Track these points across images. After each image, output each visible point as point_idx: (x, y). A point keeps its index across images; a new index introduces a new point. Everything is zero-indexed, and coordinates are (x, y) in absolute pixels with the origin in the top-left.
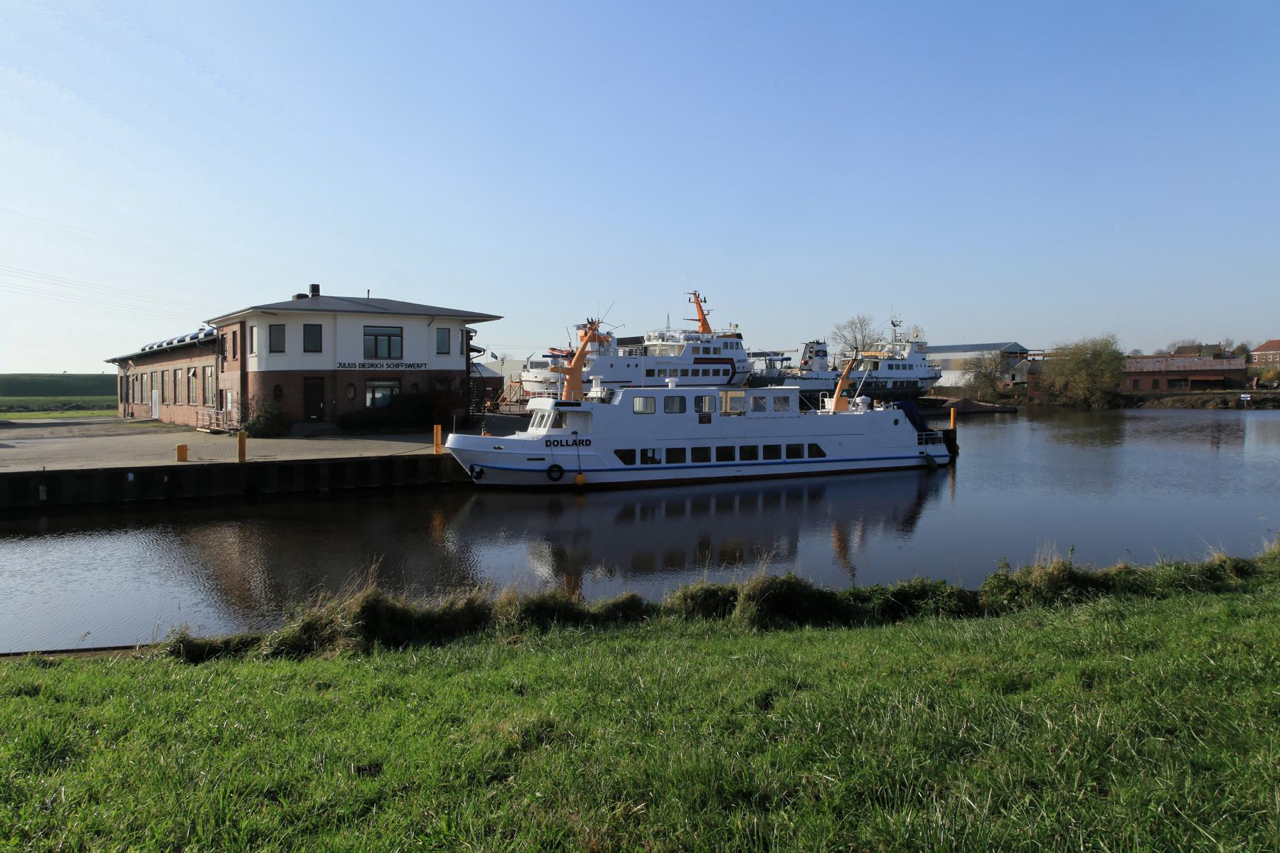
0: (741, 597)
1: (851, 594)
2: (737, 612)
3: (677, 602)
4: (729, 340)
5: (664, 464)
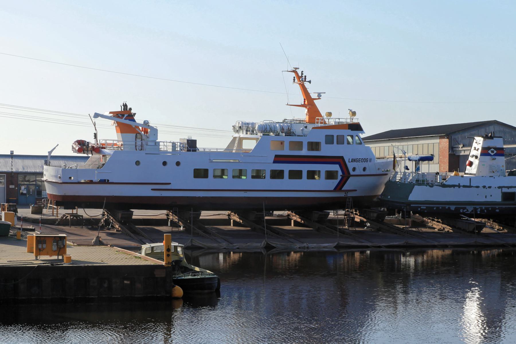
4: (335, 133)
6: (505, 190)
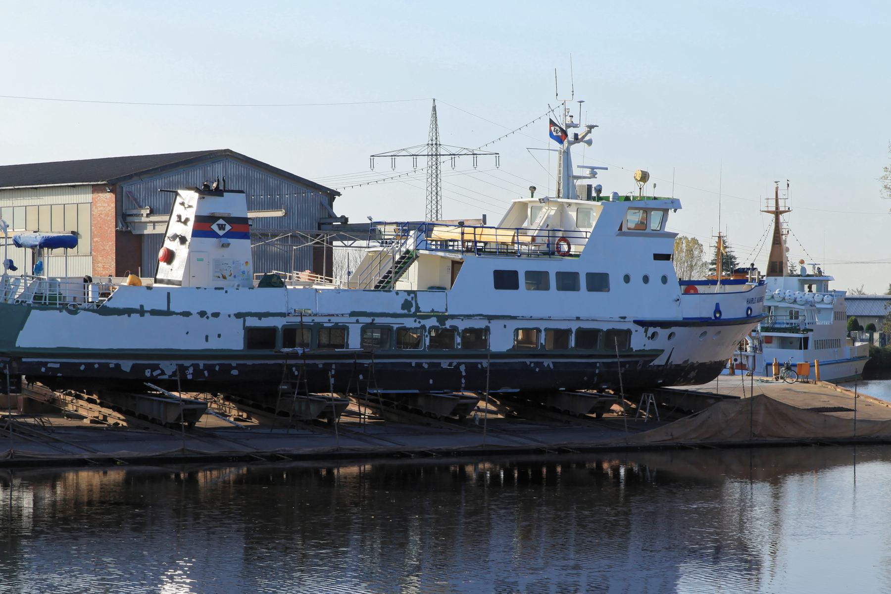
6: (252, 322)
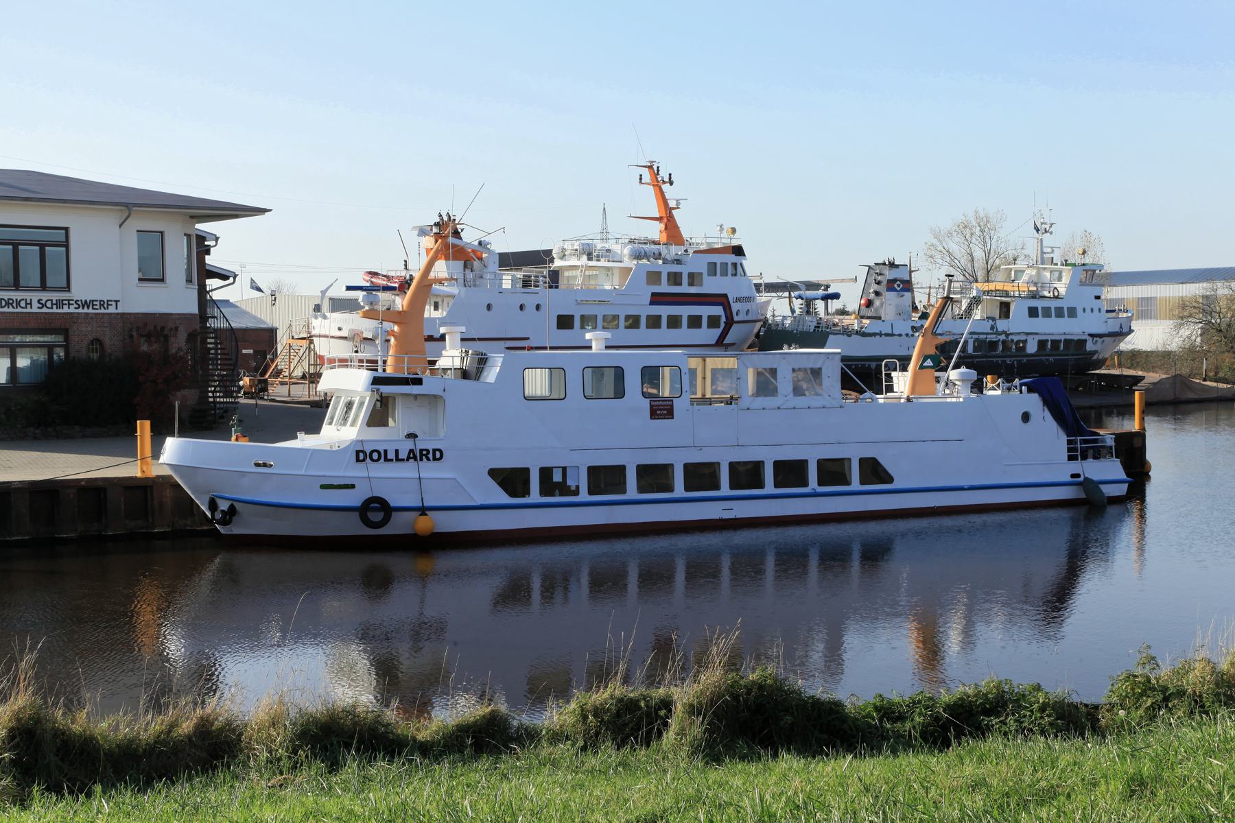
0: (679, 709)
1: (876, 708)
2: (670, 736)
3: (570, 720)
4: (718, 259)
5: (584, 496)
